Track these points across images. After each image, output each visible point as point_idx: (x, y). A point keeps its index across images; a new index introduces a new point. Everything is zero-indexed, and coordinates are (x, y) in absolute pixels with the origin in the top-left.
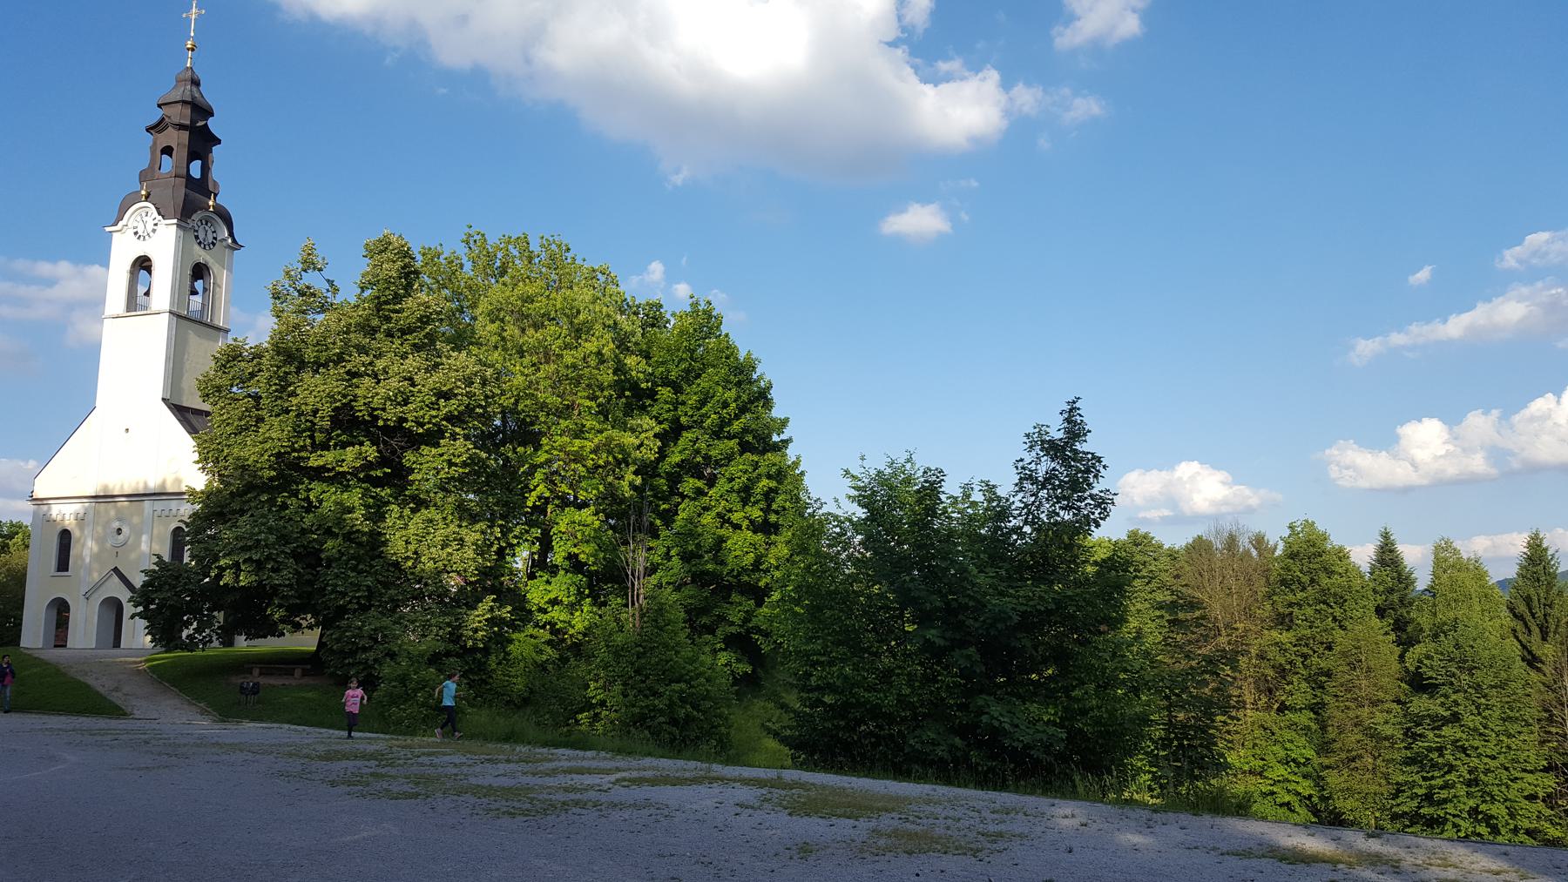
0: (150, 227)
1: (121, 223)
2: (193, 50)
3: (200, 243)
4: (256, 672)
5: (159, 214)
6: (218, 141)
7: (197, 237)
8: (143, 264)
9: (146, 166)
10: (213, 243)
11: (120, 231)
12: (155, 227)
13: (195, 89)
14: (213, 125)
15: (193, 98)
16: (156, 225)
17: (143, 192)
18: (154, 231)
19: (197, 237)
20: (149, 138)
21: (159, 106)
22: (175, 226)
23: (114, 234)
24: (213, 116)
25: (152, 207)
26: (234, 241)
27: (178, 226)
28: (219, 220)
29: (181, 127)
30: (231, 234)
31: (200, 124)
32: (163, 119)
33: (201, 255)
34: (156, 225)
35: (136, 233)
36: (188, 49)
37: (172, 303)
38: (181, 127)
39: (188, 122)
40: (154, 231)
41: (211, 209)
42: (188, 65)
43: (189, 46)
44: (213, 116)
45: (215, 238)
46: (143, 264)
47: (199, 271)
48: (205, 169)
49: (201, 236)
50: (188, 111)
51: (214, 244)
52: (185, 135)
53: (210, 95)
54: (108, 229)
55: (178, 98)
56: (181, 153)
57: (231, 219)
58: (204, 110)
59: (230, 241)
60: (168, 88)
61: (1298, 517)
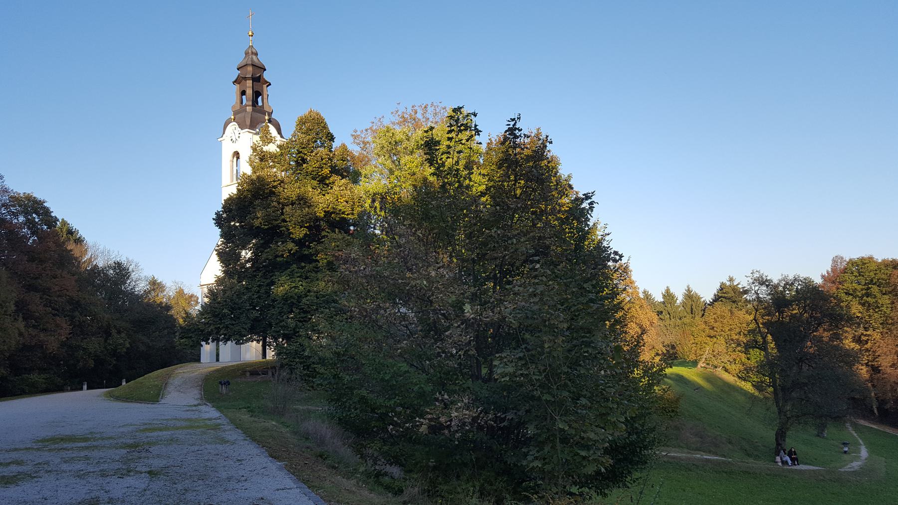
0: (237, 135)
2: (252, 36)
4: (248, 374)
12: (239, 135)
13: (254, 57)
14: (266, 76)
16: (239, 134)
17: (233, 117)
18: (239, 137)
21: (238, 69)
24: (265, 70)
27: (249, 132)
30: (279, 132)
32: (239, 75)
34: (239, 134)
35: (232, 140)
36: (250, 36)
40: (239, 137)
41: (267, 121)
42: (251, 45)
43: (250, 34)
44: (265, 70)
46: (237, 155)
50: (250, 69)
52: (249, 83)
53: (263, 59)
54: (219, 140)
56: (249, 92)
57: (279, 126)
60: (240, 59)
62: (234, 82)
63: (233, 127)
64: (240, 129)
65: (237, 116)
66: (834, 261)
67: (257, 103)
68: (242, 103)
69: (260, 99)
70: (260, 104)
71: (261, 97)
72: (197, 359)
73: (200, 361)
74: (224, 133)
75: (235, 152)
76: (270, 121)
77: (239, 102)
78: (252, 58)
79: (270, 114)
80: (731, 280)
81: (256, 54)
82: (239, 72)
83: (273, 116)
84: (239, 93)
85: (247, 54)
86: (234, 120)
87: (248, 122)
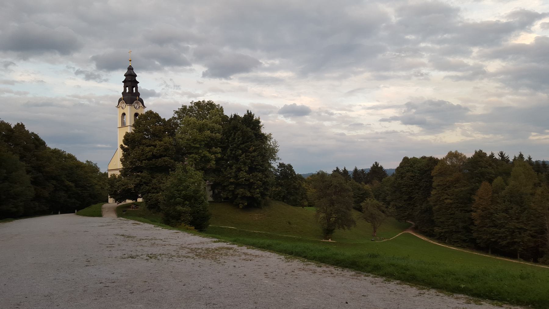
0: (124, 106)
1: (119, 106)
2: (131, 61)
3: (136, 108)
6: (139, 83)
8: (124, 114)
9: (123, 91)
10: (139, 108)
13: (132, 71)
14: (137, 79)
18: (125, 107)
19: (135, 107)
20: (123, 83)
21: (125, 76)
22: (129, 106)
24: (137, 76)
26: (144, 106)
28: (140, 102)
38: (129, 81)
39: (130, 80)
40: (125, 107)
44: (137, 76)
45: (139, 106)
46: (124, 114)
55: (128, 74)
59: (143, 106)
62: (123, 82)
64: (126, 104)
69: (134, 89)
70: (134, 91)
72: (107, 201)
75: (123, 113)
76: (139, 100)
78: (131, 72)
79: (139, 97)
80: (376, 163)
81: (132, 69)
82: (125, 77)
83: (140, 97)
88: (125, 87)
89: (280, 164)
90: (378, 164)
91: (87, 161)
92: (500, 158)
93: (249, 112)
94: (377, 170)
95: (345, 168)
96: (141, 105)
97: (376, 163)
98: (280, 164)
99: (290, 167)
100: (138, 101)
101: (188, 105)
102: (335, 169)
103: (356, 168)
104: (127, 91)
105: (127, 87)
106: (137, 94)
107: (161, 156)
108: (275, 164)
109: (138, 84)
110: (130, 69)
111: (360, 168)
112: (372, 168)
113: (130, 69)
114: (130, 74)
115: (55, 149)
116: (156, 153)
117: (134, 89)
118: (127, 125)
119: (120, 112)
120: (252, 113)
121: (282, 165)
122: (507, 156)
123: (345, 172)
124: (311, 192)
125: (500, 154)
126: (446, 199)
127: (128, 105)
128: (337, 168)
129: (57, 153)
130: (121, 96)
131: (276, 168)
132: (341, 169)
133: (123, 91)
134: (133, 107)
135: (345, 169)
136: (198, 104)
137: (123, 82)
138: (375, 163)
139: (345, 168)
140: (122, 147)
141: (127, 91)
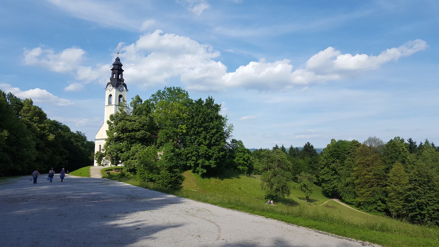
0: (111, 88)
1: (107, 89)
2: (118, 54)
3: (120, 91)
5: (113, 87)
6: (124, 71)
7: (119, 90)
8: (111, 96)
11: (107, 90)
15: (118, 63)
18: (112, 90)
19: (119, 90)
20: (111, 71)
21: (113, 65)
22: (115, 89)
23: (106, 91)
25: (111, 85)
26: (127, 90)
27: (115, 88)
29: (116, 69)
31: (120, 68)
32: (113, 68)
33: (120, 93)
37: (115, 103)
40: (112, 90)
46: (111, 96)
47: (120, 96)
48: (122, 76)
49: (120, 90)
50: (117, 66)
51: (123, 91)
52: (117, 71)
53: (121, 62)
57: (126, 85)
58: (120, 65)
59: (126, 90)
60: (114, 61)
61: (397, 136)
62: (111, 70)
63: (110, 87)
64: (112, 87)
65: (112, 82)
66: (332, 140)
67: (119, 77)
68: (113, 77)
69: (120, 75)
70: (120, 78)
71: (120, 75)
72: (93, 164)
73: (93, 165)
74: (106, 88)
75: (110, 95)
76: (123, 85)
77: (113, 77)
79: (123, 81)
80: (308, 143)
81: (119, 60)
83: (124, 82)
84: (113, 74)
85: (116, 60)
86: (111, 83)
87: (116, 85)
88: (113, 74)
89: (233, 140)
90: (310, 144)
91: (77, 132)
92: (409, 143)
93: (210, 97)
94: (308, 148)
95: (283, 145)
96: (125, 89)
97: (308, 143)
98: (233, 140)
99: (240, 143)
100: (123, 86)
101: (163, 90)
102: (275, 146)
103: (292, 147)
104: (114, 77)
105: (114, 74)
106: (122, 80)
107: (139, 130)
108: (228, 141)
109: (123, 72)
110: (118, 59)
111: (294, 146)
112: (305, 146)
113: (118, 59)
114: (117, 64)
115: (54, 121)
116: (135, 128)
117: (120, 75)
118: (112, 104)
119: (108, 93)
120: (213, 99)
121: (234, 141)
122: (415, 142)
123: (283, 149)
124: (257, 165)
125: (409, 141)
126: (366, 174)
127: (114, 89)
128: (276, 145)
129: (56, 125)
130: (110, 81)
131: (230, 143)
132: (280, 146)
133: (110, 75)
134: (119, 90)
135: (283, 146)
136: (169, 90)
137: (111, 70)
138: (307, 143)
139: (283, 145)
140: (108, 122)
141: (114, 77)
